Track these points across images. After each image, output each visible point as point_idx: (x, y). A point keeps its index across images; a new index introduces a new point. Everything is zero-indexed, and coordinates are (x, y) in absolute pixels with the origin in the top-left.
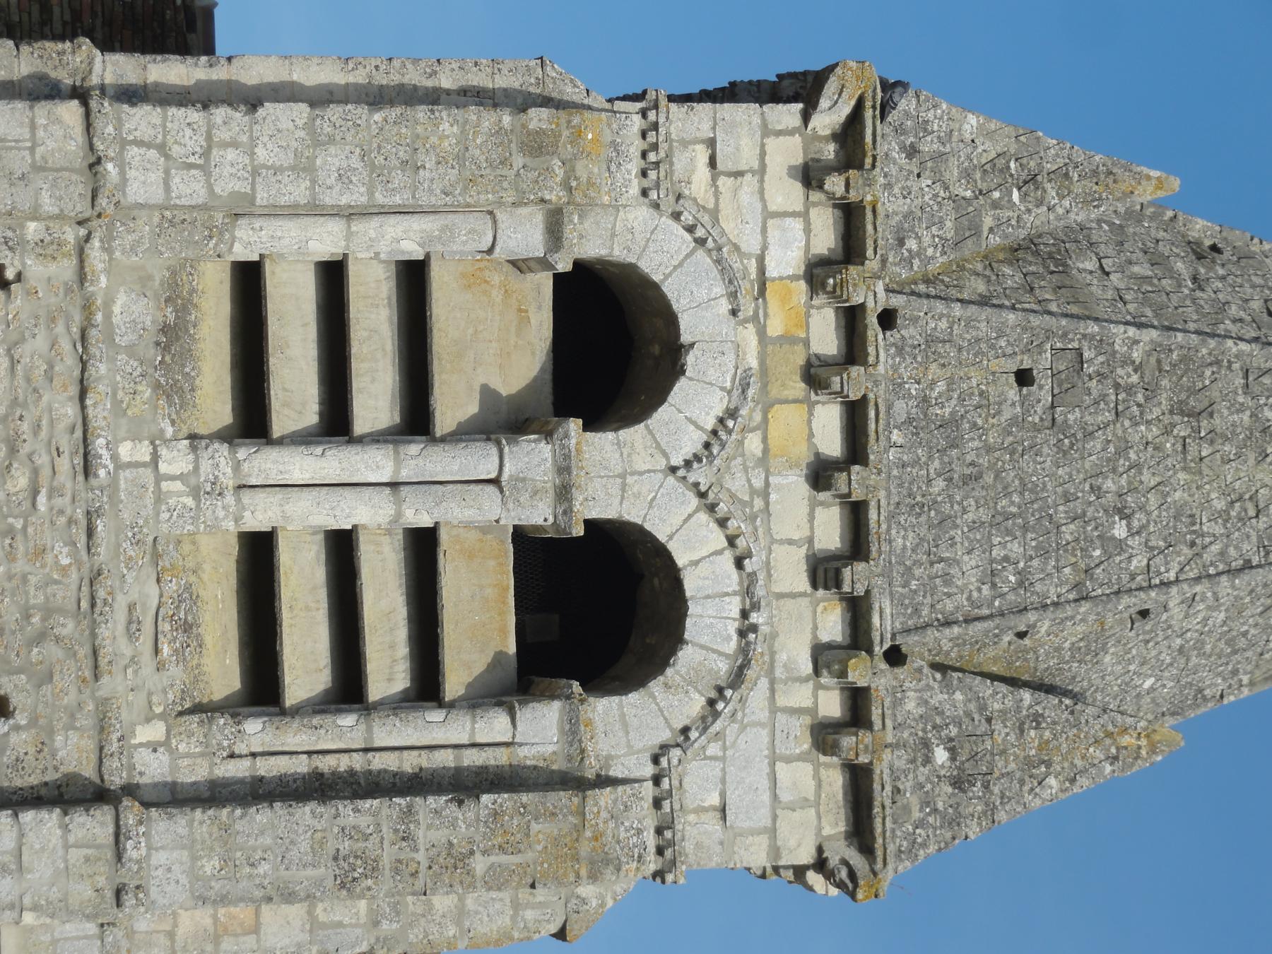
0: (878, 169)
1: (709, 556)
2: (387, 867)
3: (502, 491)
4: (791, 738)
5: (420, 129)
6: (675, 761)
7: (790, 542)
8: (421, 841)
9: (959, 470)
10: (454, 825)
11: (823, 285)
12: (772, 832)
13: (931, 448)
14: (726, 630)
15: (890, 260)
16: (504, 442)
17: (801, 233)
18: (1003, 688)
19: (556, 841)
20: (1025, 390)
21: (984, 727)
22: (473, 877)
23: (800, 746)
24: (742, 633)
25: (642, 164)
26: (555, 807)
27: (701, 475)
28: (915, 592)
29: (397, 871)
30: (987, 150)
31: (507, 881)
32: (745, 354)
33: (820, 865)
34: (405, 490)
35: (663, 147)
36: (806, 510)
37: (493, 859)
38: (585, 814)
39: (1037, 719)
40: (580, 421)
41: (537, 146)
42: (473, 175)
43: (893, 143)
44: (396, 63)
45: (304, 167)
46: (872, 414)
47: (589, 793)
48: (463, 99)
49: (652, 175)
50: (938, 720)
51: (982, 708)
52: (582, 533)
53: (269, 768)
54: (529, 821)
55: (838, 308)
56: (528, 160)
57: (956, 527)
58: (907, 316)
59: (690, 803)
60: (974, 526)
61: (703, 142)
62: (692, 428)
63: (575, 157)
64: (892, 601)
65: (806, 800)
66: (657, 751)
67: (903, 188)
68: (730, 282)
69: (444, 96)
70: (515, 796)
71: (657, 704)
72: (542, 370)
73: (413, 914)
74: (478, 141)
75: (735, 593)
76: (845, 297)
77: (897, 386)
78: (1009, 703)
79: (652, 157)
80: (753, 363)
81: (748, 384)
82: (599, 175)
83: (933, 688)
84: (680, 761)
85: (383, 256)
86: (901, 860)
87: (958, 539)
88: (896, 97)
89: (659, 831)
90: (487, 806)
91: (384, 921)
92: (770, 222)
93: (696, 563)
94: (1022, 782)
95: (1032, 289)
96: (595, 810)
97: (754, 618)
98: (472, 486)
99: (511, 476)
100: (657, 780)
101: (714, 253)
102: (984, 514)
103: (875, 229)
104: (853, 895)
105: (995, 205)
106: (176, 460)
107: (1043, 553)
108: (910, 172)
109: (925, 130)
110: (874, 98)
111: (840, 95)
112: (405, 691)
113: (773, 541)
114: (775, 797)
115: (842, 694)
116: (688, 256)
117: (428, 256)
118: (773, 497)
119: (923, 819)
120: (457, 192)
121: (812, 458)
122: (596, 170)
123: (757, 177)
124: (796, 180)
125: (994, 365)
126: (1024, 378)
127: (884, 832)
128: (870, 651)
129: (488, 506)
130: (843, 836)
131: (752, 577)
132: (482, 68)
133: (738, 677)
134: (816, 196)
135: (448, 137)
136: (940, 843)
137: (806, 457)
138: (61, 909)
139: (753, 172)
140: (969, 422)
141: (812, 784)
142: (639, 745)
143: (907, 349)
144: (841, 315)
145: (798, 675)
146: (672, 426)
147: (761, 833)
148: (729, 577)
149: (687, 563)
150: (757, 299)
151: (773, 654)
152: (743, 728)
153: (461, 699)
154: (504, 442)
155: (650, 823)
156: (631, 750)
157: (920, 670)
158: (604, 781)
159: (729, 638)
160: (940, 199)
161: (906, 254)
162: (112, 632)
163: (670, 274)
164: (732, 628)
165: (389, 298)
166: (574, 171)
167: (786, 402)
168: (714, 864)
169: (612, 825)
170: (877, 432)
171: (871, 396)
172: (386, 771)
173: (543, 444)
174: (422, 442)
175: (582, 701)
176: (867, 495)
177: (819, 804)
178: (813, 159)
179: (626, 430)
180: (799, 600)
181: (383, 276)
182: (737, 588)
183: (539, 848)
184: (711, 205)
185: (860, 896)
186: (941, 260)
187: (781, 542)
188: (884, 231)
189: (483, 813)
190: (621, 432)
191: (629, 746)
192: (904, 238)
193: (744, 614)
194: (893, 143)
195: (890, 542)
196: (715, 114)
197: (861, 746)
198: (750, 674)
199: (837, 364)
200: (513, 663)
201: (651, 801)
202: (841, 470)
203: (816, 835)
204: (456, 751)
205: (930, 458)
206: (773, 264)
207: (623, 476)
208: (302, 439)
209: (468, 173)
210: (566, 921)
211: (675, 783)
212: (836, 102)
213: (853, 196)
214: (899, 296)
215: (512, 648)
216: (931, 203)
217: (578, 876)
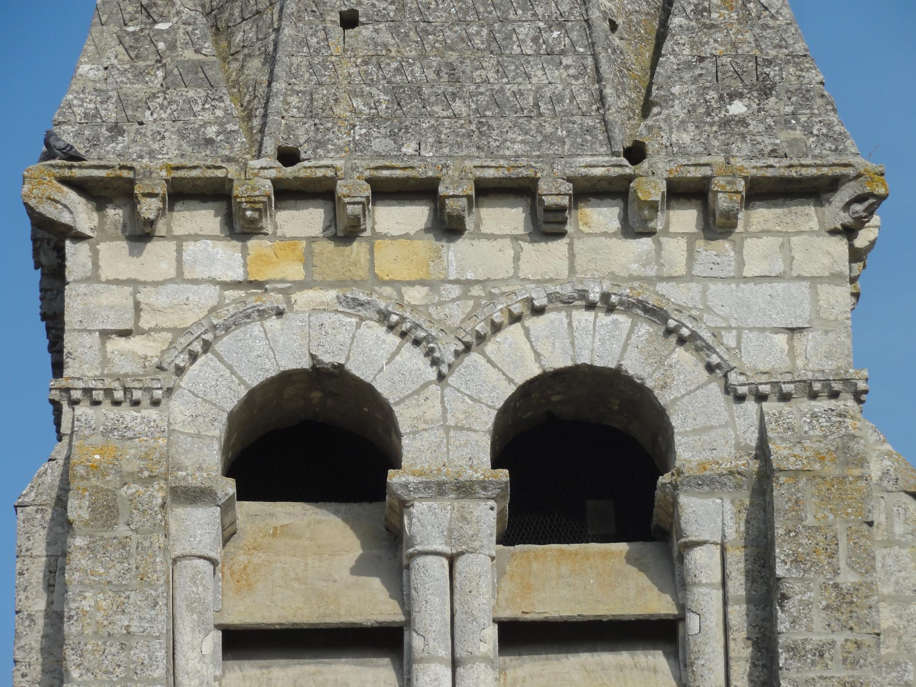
0: (135, 164)
1: (531, 342)
2: (851, 673)
3: (462, 553)
4: (718, 260)
5: (88, 631)
6: (742, 379)
7: (517, 258)
8: (824, 638)
9: (444, 86)
10: (808, 604)
11: (253, 221)
12: (814, 280)
13: (421, 114)
14: (607, 325)
15: (227, 153)
16: (411, 550)
17: (198, 244)
18: (668, 45)
19: (825, 500)
20: (361, 19)
21: (709, 65)
22: (861, 585)
23: (727, 251)
24: (611, 309)
25: (126, 405)
26: (790, 500)
27: (447, 349)
28: (569, 132)
29: (855, 663)
30: (115, 54)
31: (865, 550)
32: (322, 303)
33: (849, 232)
34: (460, 653)
35: (109, 383)
36: (484, 243)
37: (842, 564)
38: (797, 470)
39: (700, 11)
40: (391, 472)
42: (136, 577)
43: (108, 149)
44: (19, 656)
46: (386, 173)
47: (775, 465)
48: (57, 587)
49: (137, 395)
50: (702, 110)
51: (689, 66)
52: (506, 471)
54: (804, 527)
55: (276, 207)
56: (122, 520)
57: (502, 90)
58: (285, 137)
59: (786, 364)
60: (501, 70)
61: (103, 344)
62: (398, 358)
63: (119, 472)
64: (579, 155)
65: (782, 246)
66: (731, 397)
67: (154, 139)
68: (248, 317)
69: (55, 607)
70: (778, 541)
71: (683, 396)
72: (336, 513)
73: (898, 648)
74: (101, 571)
75: (569, 316)
76: (265, 199)
77: (357, 147)
78: (683, 39)
79: (119, 395)
80: (332, 294)
81: (354, 299)
82: (137, 448)
83: (668, 115)
84: (742, 374)
85: (218, 673)
86: (845, 149)
87: (515, 88)
88: (60, 145)
89: (814, 396)
90: (788, 570)
91: (906, 678)
92: (188, 275)
93: (538, 355)
94: (765, 27)
95: (258, 12)
96: (792, 459)
97: (594, 296)
98: (457, 583)
99: (446, 544)
100: (761, 398)
101: (218, 333)
102: (490, 62)
103: (195, 167)
104: (881, 198)
105: (172, 46)
108: (137, 132)
109: (94, 116)
110: (60, 167)
111: (57, 202)
112: (666, 655)
113: (516, 276)
114: (779, 277)
115: (674, 208)
116: (221, 360)
117: (218, 627)
118: (470, 276)
119: (803, 126)
120: (154, 593)
121: (431, 235)
122: (132, 451)
123: (141, 289)
124: (144, 248)
125: (337, 49)
127: (816, 166)
128: (630, 178)
130: (819, 209)
131: (551, 297)
132: (25, 568)
133: (656, 314)
134: (161, 228)
135: (97, 602)
136: (827, 110)
137: (429, 243)
139: (136, 292)
140: (395, 76)
141: (766, 239)
142: (725, 416)
143: (319, 136)
144: (284, 204)
145: (654, 253)
146: (396, 378)
147: (817, 294)
148: (552, 322)
149: (537, 365)
150: (266, 290)
151: (632, 278)
152: (708, 309)
153: (675, 598)
154: (411, 550)
155: (806, 405)
156: (730, 423)
157: (650, 128)
158: (763, 450)
159: (615, 322)
160: (165, 103)
161: (221, 137)
163: (239, 378)
164: (605, 319)
165: (261, 667)
166: (133, 474)
167: (372, 262)
168: (848, 342)
169: (807, 443)
170: (404, 168)
171: (367, 174)
172: (750, 675)
173: (414, 510)
174: (410, 636)
175: (680, 473)
176: (469, 179)
177: (787, 232)
178: (123, 231)
179: (400, 425)
180: (576, 250)
181: (239, 673)
182: (564, 314)
183: (831, 517)
184: (169, 336)
185: (881, 191)
186: (228, 102)
187: (516, 268)
188: (197, 159)
189: (795, 574)
190: (402, 430)
191: (726, 425)
192: (205, 139)
193: (591, 306)
194: (107, 149)
195: (518, 156)
196: (75, 330)
197: (728, 188)
198: (652, 301)
199: (334, 209)
200: (638, 545)
201: (782, 404)
202: (443, 206)
203: (818, 236)
204: (730, 602)
205: (431, 115)
206: (230, 273)
207: (447, 429)
209: (134, 582)
210: (906, 492)
211: (764, 378)
212: (65, 206)
213: (162, 189)
214: (264, 145)
215: (622, 547)
216: (169, 111)
217: (861, 478)
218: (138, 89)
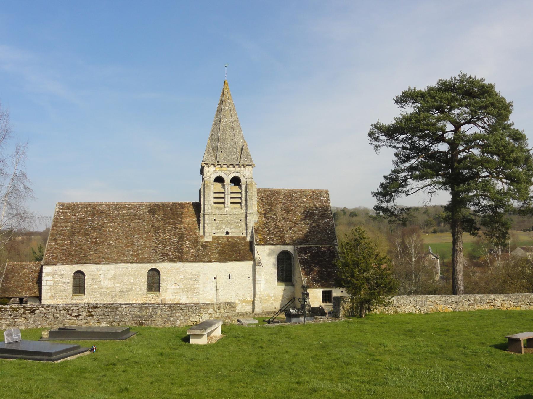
30: (207, 154)
41: (207, 186)
45: (209, 201)
53: (245, 204)
77: (222, 161)
106: (226, 209)
107: (233, 151)
126: (222, 152)
129: (229, 189)
133: (241, 173)
138: (253, 217)
162: (237, 213)
208: (225, 200)
218: (208, 157)
